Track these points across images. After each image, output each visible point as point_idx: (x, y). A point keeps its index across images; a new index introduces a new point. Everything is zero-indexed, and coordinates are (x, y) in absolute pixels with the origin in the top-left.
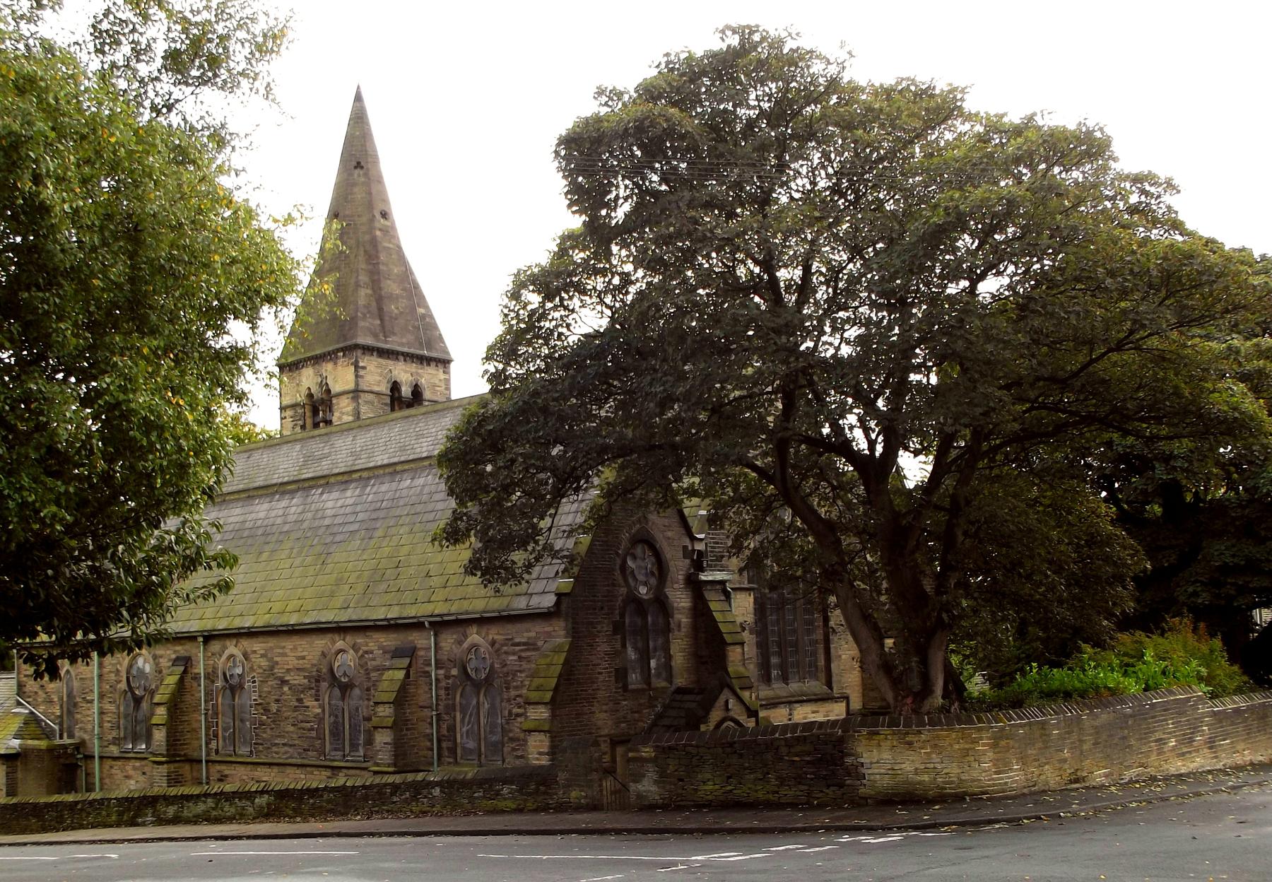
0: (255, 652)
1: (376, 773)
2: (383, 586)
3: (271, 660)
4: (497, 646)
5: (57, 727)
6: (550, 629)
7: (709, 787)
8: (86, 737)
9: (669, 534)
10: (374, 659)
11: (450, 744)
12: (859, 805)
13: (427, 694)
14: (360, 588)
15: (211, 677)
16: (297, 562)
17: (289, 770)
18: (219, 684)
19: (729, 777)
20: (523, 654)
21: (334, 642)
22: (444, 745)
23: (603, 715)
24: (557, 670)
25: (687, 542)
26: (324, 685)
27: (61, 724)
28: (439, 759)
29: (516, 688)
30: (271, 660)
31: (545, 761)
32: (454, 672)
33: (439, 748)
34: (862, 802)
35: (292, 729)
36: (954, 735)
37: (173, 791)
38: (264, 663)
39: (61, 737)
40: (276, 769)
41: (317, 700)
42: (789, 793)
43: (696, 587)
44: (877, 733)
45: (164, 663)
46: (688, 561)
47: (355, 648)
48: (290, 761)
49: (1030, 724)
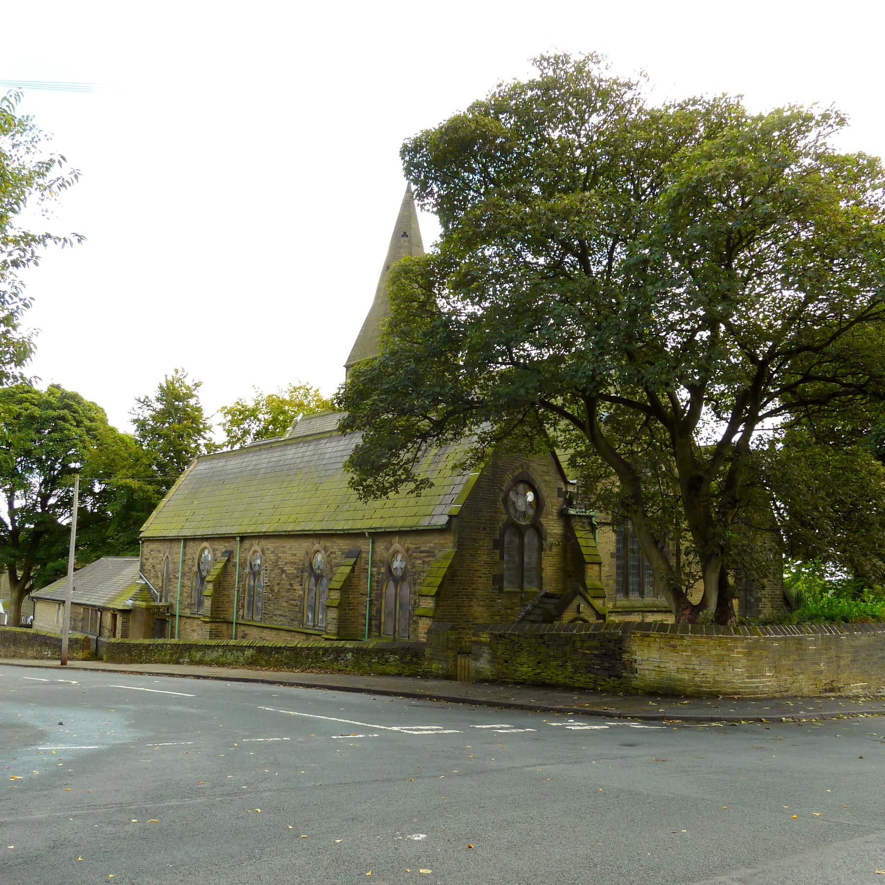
0: (268, 549)
1: (326, 639)
2: (346, 507)
3: (276, 555)
4: (410, 552)
5: (158, 594)
7: (524, 669)
8: (174, 602)
9: (547, 478)
10: (336, 558)
12: (631, 694)
13: (366, 585)
14: (335, 506)
15: (242, 565)
16: (302, 489)
17: (282, 633)
18: (247, 570)
19: (539, 663)
20: (426, 559)
21: (314, 545)
22: (373, 623)
23: (480, 609)
24: (443, 572)
25: (562, 485)
26: (306, 575)
27: (161, 592)
29: (420, 584)
30: (276, 555)
31: (425, 640)
32: (383, 570)
34: (634, 692)
35: (285, 604)
36: (712, 643)
37: (213, 642)
38: (273, 557)
39: (161, 601)
40: (274, 632)
41: (301, 585)
42: (582, 679)
44: (648, 636)
45: (219, 554)
46: (561, 499)
47: (325, 549)
48: (282, 627)
49: (785, 639)
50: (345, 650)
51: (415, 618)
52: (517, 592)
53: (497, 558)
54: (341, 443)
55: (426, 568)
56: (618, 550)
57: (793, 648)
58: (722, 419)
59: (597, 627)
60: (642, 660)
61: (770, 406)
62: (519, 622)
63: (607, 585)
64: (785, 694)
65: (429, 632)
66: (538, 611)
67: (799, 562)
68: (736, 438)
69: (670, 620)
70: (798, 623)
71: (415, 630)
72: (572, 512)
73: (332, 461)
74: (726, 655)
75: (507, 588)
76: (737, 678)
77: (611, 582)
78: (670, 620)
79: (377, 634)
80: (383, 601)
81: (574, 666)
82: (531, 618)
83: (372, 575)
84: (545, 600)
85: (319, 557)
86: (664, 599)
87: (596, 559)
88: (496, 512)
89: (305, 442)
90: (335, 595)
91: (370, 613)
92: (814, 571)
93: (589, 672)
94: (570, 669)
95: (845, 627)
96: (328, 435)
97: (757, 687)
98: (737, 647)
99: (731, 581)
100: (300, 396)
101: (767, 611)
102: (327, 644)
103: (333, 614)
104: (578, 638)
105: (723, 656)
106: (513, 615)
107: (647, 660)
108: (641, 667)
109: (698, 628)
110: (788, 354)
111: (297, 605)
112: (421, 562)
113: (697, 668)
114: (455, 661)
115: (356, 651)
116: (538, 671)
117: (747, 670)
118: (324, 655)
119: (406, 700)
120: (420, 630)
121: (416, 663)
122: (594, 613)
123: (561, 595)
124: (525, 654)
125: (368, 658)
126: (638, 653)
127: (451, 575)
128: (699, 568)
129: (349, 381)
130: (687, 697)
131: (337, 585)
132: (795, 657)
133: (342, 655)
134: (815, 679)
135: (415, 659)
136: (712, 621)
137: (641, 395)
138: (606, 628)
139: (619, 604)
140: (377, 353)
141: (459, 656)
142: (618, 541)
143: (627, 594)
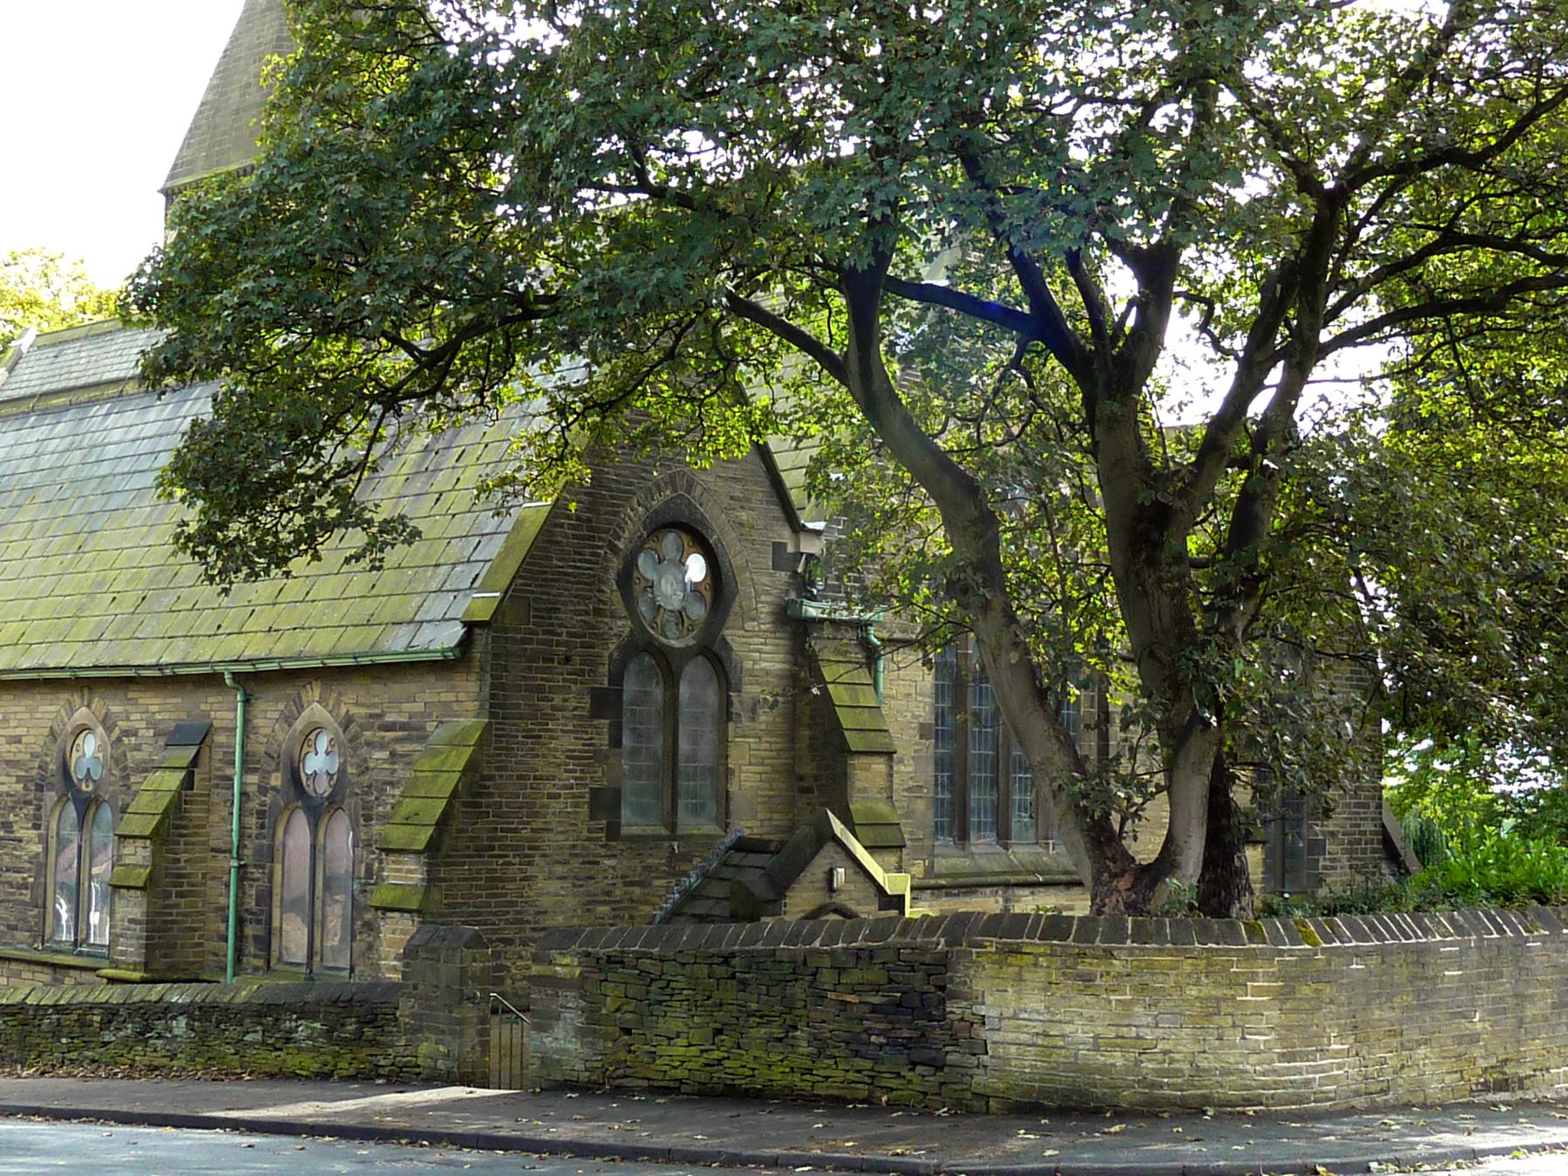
1: (112, 981)
2: (168, 600)
4: (354, 728)
6: (450, 697)
7: (679, 1049)
9: (743, 516)
10: (137, 748)
11: (259, 930)
12: (971, 1112)
13: (226, 824)
14: (131, 599)
16: (35, 550)
19: (719, 1032)
20: (399, 748)
21: (72, 711)
22: (250, 930)
23: (554, 886)
24: (448, 783)
25: (784, 535)
26: (51, 796)
28: (238, 960)
29: (384, 818)
31: (396, 977)
32: (276, 780)
33: (240, 937)
34: (977, 1104)
36: (1187, 966)
41: (36, 827)
42: (837, 1074)
43: (796, 629)
44: (1017, 951)
46: (783, 576)
47: (107, 722)
49: (1383, 952)
50: (167, 1011)
51: (368, 916)
52: (657, 838)
53: (603, 741)
54: (152, 414)
55: (402, 772)
56: (940, 716)
57: (1402, 974)
58: (1227, 353)
59: (880, 930)
60: (1001, 1018)
61: (1354, 316)
62: (666, 920)
63: (909, 814)
64: (1379, 1099)
65: (410, 953)
66: (718, 890)
67: (1427, 743)
68: (1259, 405)
69: (1079, 906)
70: (1417, 909)
71: (370, 947)
72: (812, 610)
73: (125, 466)
74: (1225, 999)
75: (631, 823)
76: (1253, 1059)
77: (920, 805)
78: (1079, 906)
79: (260, 963)
80: (278, 867)
81: (815, 1039)
82: (700, 908)
83: (243, 794)
84: (736, 858)
85: (89, 745)
86: (1062, 849)
87: (878, 742)
88: (598, 612)
89: (45, 412)
90: (138, 854)
91: (239, 904)
92: (1465, 766)
93: (857, 1054)
94: (804, 1048)
95: (1539, 916)
96: (112, 391)
97: (1307, 1083)
98: (1253, 977)
99: (1241, 796)
100: (27, 278)
101: (1338, 878)
102: (114, 995)
103: (133, 908)
104: (827, 962)
105: (1218, 1000)
106: (647, 903)
107: (1015, 1017)
108: (997, 1037)
109: (1151, 928)
110: (1404, 171)
111: (24, 886)
112: (385, 755)
113: (1149, 1035)
114: (484, 1033)
115: (199, 1013)
116: (716, 1055)
117: (1281, 1039)
118: (105, 1025)
119: (342, 1145)
120: (384, 949)
121: (373, 1043)
122: (872, 891)
123: (782, 843)
124: (678, 1009)
125: (232, 1032)
126: (989, 999)
127: (473, 793)
128: (1157, 762)
129: (173, 235)
130: (1120, 1115)
131: (146, 826)
132: (1409, 999)
133: (160, 1025)
134: (1459, 1057)
135: (369, 1032)
136: (1191, 907)
137: (1005, 287)
138: (903, 933)
139: (942, 864)
140: (248, 156)
141: (496, 1019)
142: (939, 692)
143: (963, 837)
